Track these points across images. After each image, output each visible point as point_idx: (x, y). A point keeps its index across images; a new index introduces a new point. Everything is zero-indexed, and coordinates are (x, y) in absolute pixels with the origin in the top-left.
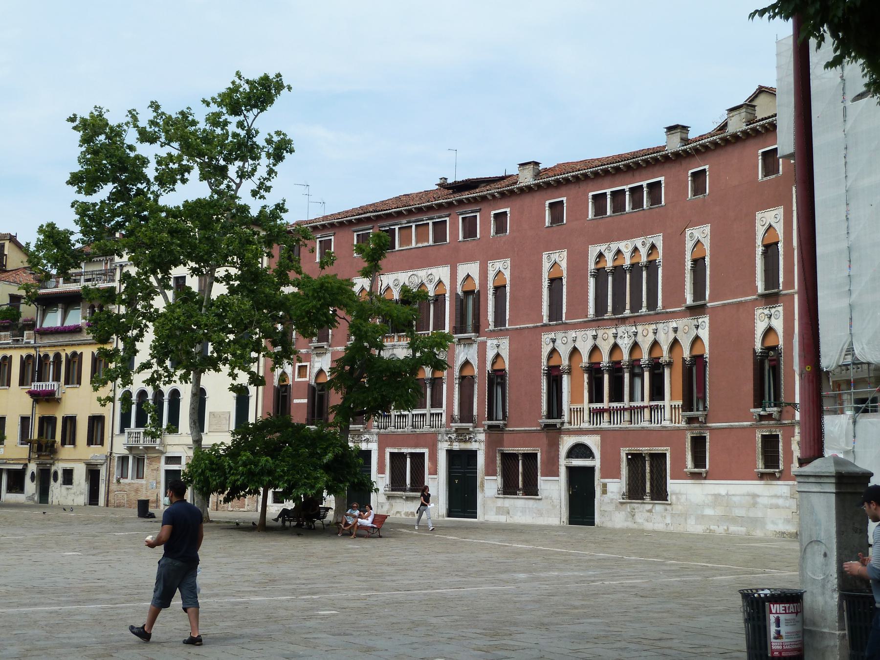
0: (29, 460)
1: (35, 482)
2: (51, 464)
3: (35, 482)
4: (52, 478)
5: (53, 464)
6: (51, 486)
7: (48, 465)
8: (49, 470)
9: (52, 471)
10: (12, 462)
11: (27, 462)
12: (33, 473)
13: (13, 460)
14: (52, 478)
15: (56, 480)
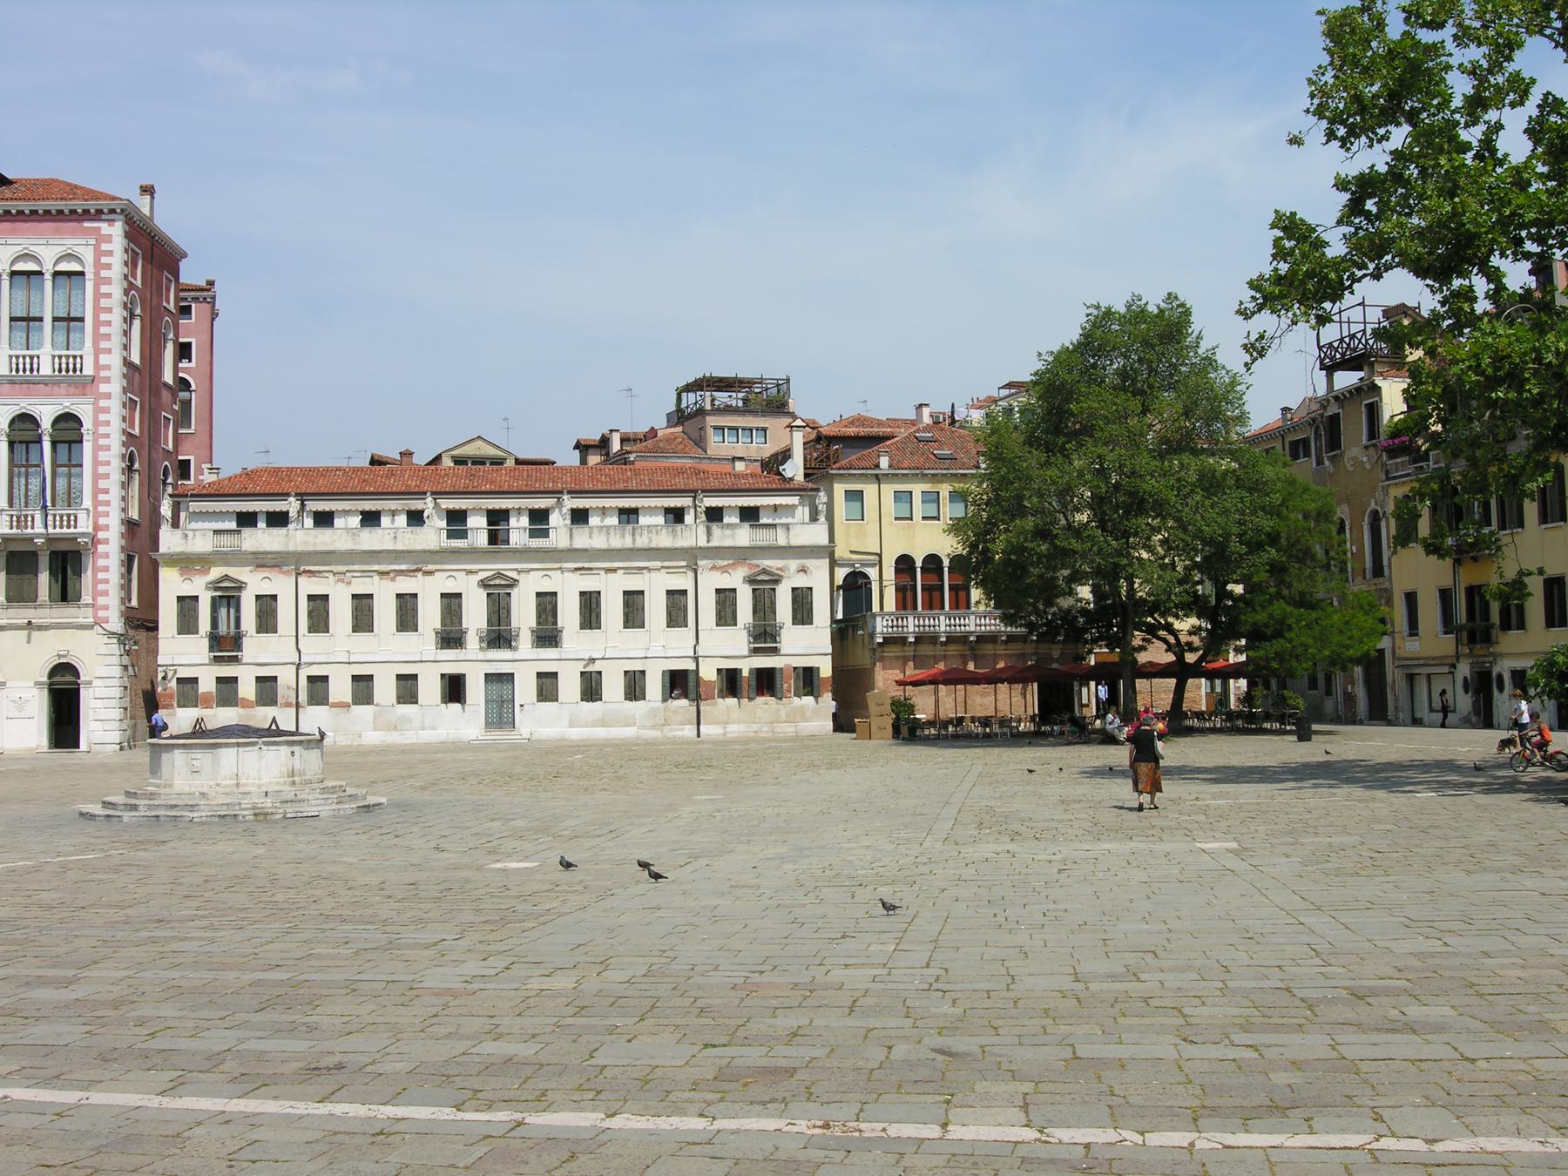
0: (1458, 656)
1: (1470, 694)
2: (1491, 663)
3: (1470, 694)
4: (1495, 686)
5: (1495, 661)
6: (1495, 698)
7: (1488, 665)
8: (1489, 673)
9: (1494, 674)
10: (1432, 662)
11: (1454, 661)
12: (1465, 678)
13: (1433, 659)
14: (1495, 686)
15: (1501, 688)
